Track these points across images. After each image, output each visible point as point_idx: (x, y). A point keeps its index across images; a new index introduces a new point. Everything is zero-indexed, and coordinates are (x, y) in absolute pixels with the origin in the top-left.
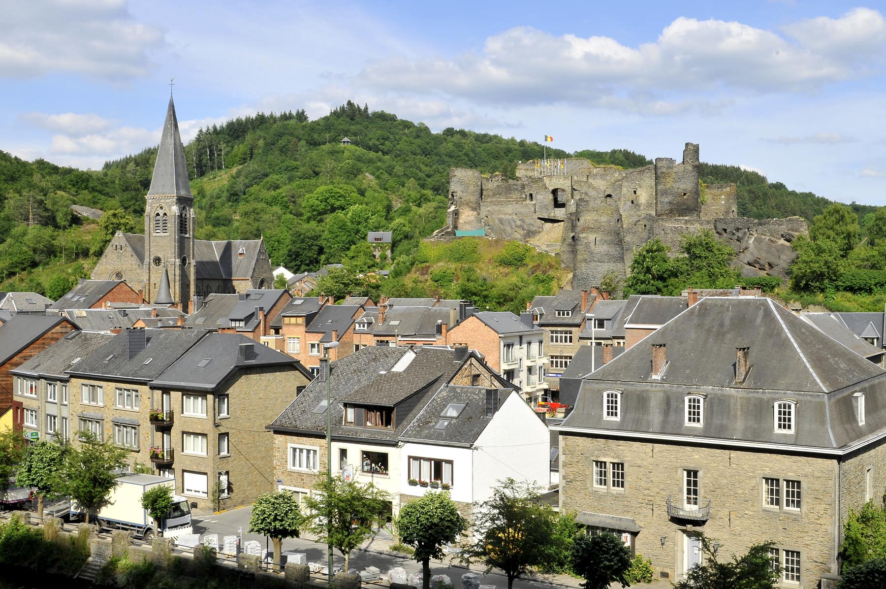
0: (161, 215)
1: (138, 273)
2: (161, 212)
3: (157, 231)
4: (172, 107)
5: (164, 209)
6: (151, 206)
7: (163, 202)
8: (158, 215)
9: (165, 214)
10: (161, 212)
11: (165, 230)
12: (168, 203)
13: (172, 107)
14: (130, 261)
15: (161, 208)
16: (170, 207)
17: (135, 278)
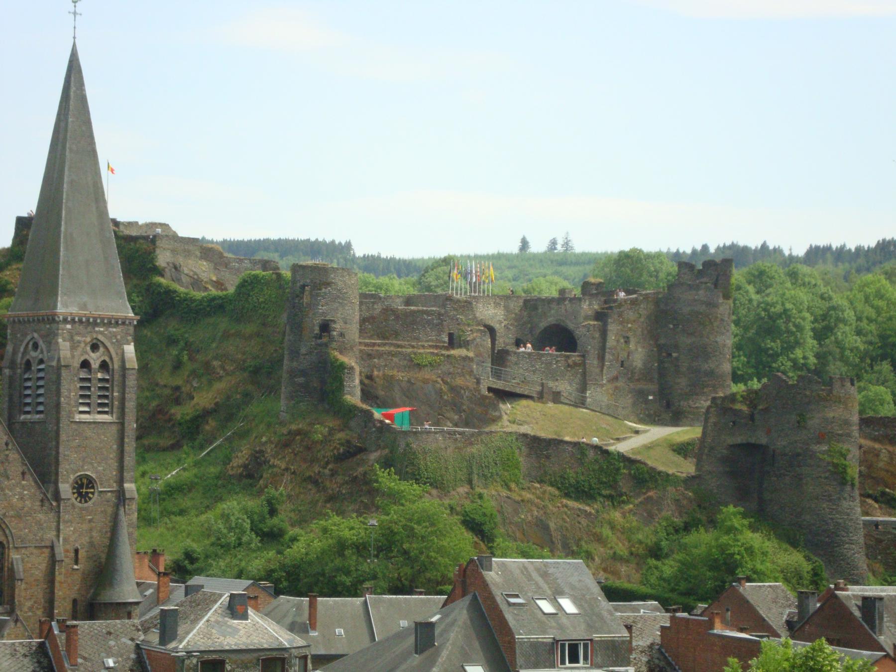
0: (95, 365)
1: (39, 523)
2: (95, 359)
3: (82, 409)
4: (74, 70)
5: (102, 349)
6: (71, 339)
7: (101, 332)
8: (85, 364)
9: (104, 366)
10: (95, 359)
11: (103, 407)
12: (115, 335)
13: (74, 70)
14: (18, 490)
15: (95, 347)
16: (119, 344)
17: (31, 536)
